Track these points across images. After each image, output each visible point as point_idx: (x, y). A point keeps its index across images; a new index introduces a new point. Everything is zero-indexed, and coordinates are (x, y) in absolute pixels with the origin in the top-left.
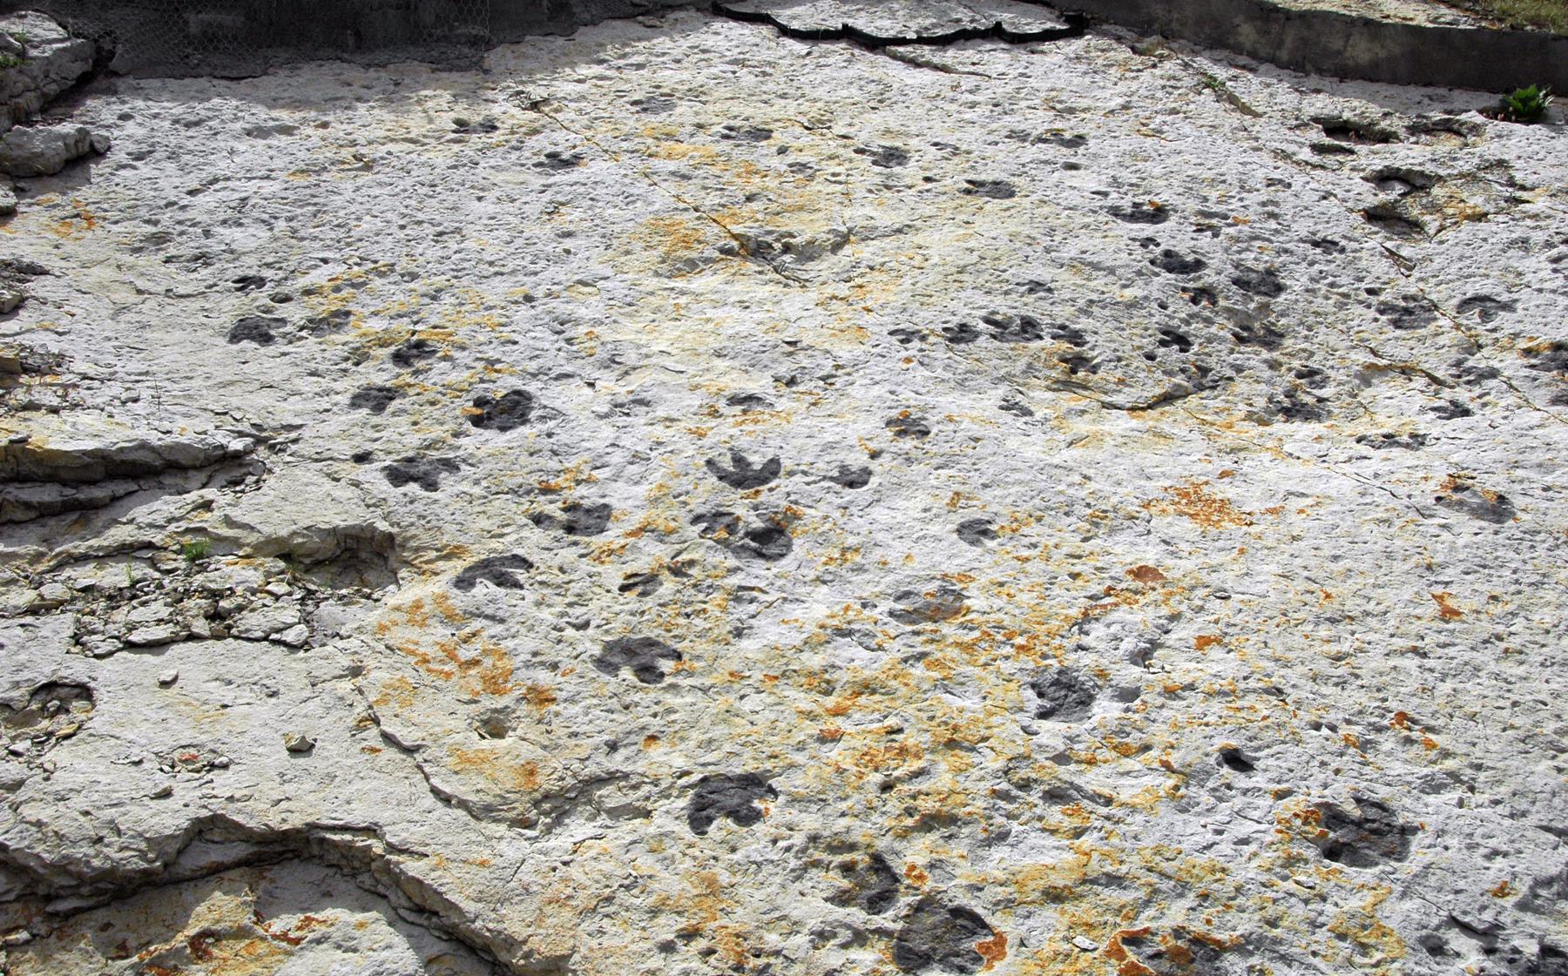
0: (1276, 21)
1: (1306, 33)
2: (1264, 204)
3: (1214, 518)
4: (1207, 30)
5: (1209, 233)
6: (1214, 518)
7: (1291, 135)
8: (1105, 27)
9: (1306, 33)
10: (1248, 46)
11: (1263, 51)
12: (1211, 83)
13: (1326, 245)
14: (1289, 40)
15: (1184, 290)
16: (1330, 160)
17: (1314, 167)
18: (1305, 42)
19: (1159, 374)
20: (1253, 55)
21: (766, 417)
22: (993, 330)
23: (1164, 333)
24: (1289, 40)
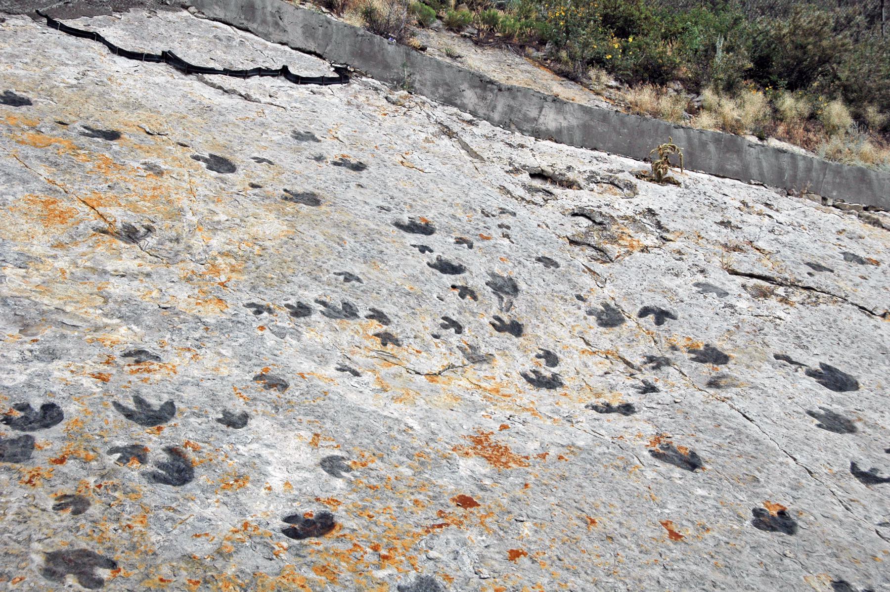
0: (491, 90)
1: (512, 103)
2: (500, 226)
3: (503, 460)
4: (441, 90)
5: (465, 245)
6: (503, 460)
7: (509, 177)
8: (364, 79)
9: (512, 103)
10: (471, 107)
11: (481, 112)
12: (449, 133)
13: (547, 262)
14: (500, 108)
15: (454, 287)
16: (539, 198)
17: (528, 202)
18: (511, 108)
19: (444, 350)
20: (474, 113)
21: (157, 368)
22: (322, 308)
23: (443, 318)
24: (500, 108)
